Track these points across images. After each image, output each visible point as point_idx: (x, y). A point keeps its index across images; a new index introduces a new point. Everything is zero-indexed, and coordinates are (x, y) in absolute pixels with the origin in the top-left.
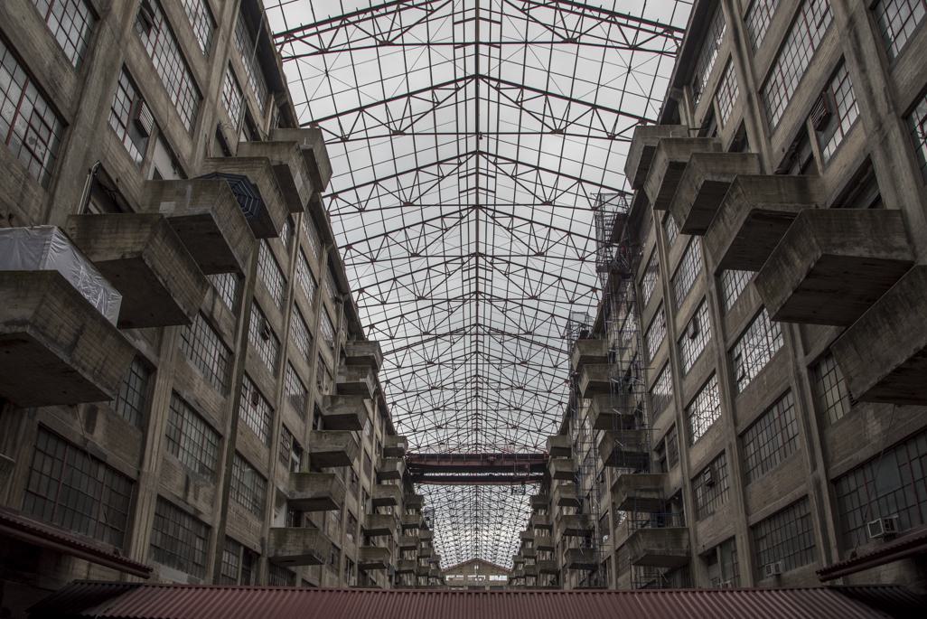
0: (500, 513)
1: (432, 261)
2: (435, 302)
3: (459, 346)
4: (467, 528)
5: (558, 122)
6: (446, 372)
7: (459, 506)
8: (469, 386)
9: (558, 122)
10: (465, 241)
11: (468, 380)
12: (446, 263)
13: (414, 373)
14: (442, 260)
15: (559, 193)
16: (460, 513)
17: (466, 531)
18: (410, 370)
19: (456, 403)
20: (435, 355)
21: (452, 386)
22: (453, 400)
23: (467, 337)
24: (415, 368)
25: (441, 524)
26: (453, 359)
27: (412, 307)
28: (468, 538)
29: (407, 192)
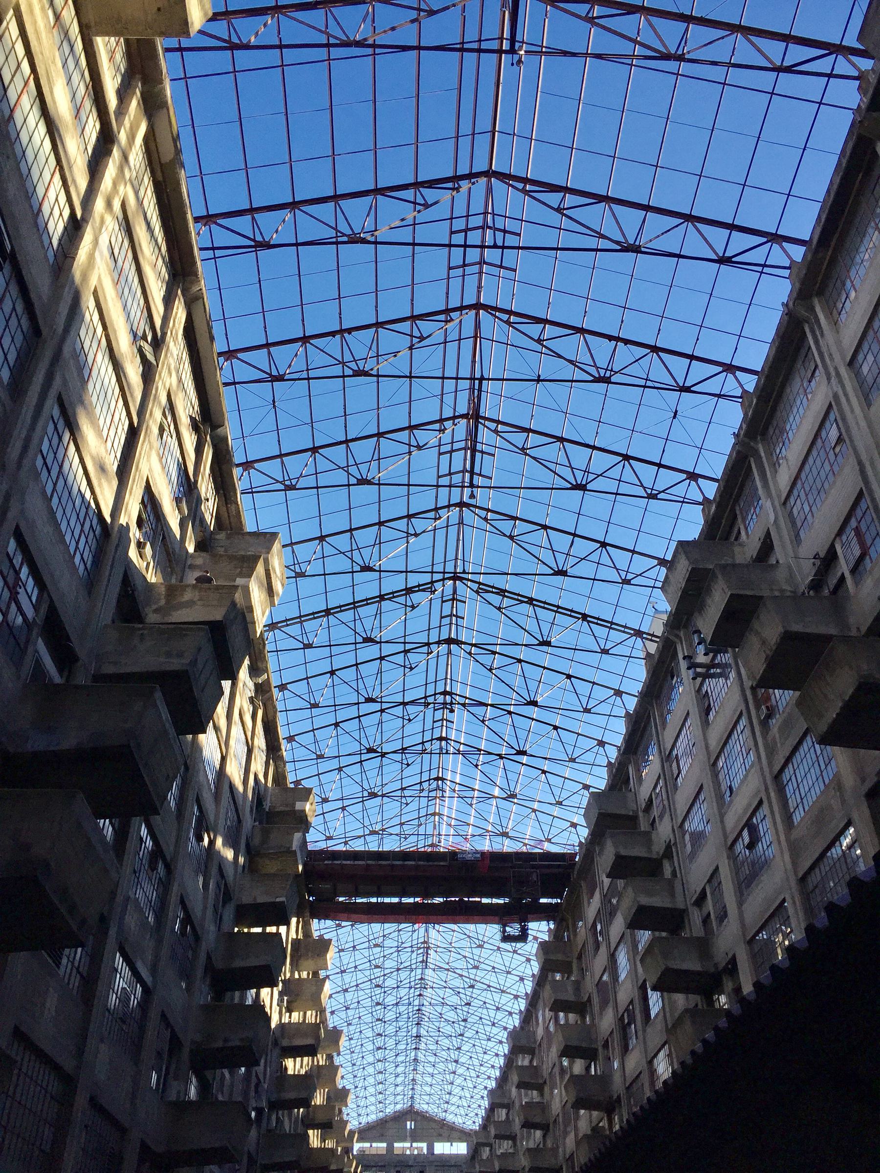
0: (456, 1042)
1: (387, 649)
2: (385, 706)
3: (414, 727)
4: (400, 1059)
5: (561, 558)
6: (392, 768)
7: (390, 1015)
8: (425, 794)
9: (561, 558)
10: (439, 558)
11: (425, 785)
12: (406, 652)
13: (343, 809)
14: (401, 648)
15: (591, 477)
16: (391, 1030)
17: (397, 1076)
18: (339, 804)
19: (402, 824)
20: (378, 742)
21: (396, 830)
22: (397, 821)
23: (429, 711)
24: (346, 803)
25: (357, 1050)
26: (403, 789)
27: (353, 712)
28: (399, 1080)
29: (364, 468)
